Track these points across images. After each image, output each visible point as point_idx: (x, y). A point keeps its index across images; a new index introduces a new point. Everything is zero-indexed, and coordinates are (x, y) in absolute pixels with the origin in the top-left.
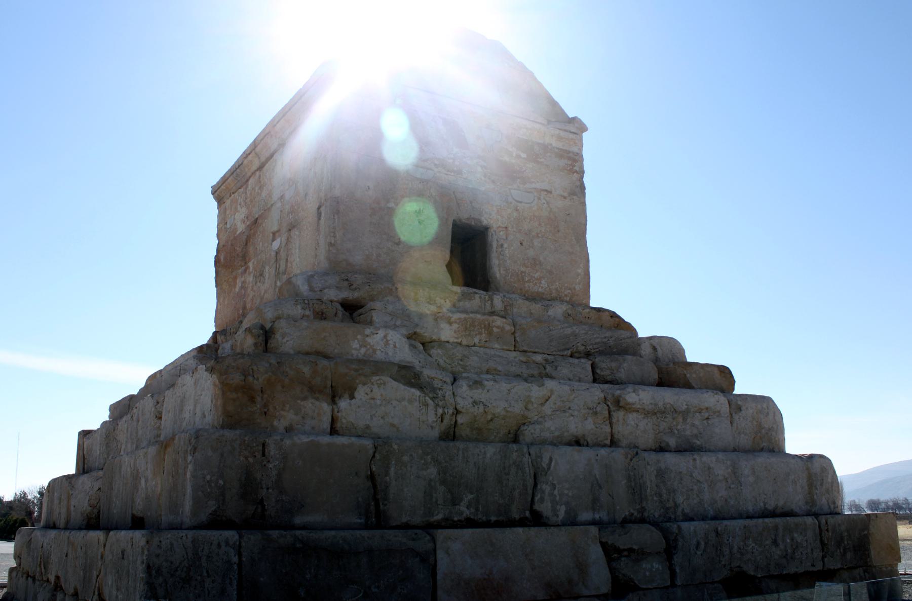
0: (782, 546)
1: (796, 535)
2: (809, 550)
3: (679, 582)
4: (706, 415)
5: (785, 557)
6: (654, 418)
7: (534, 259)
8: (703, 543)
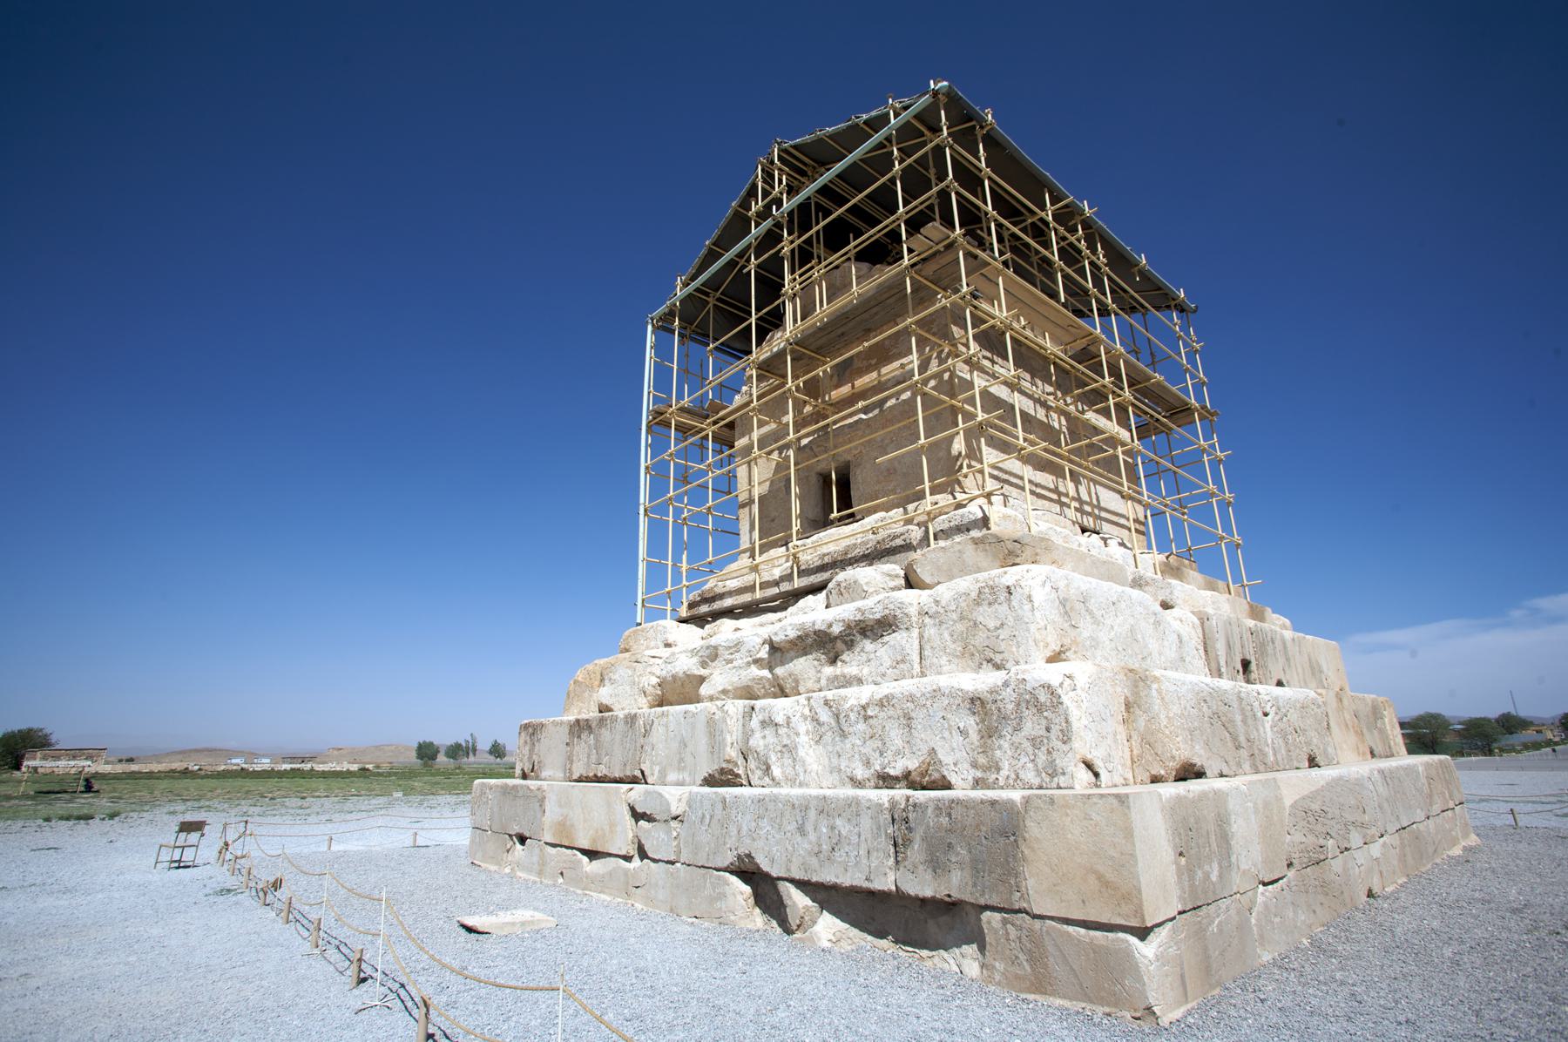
0: (812, 837)
1: (839, 822)
5: (817, 854)
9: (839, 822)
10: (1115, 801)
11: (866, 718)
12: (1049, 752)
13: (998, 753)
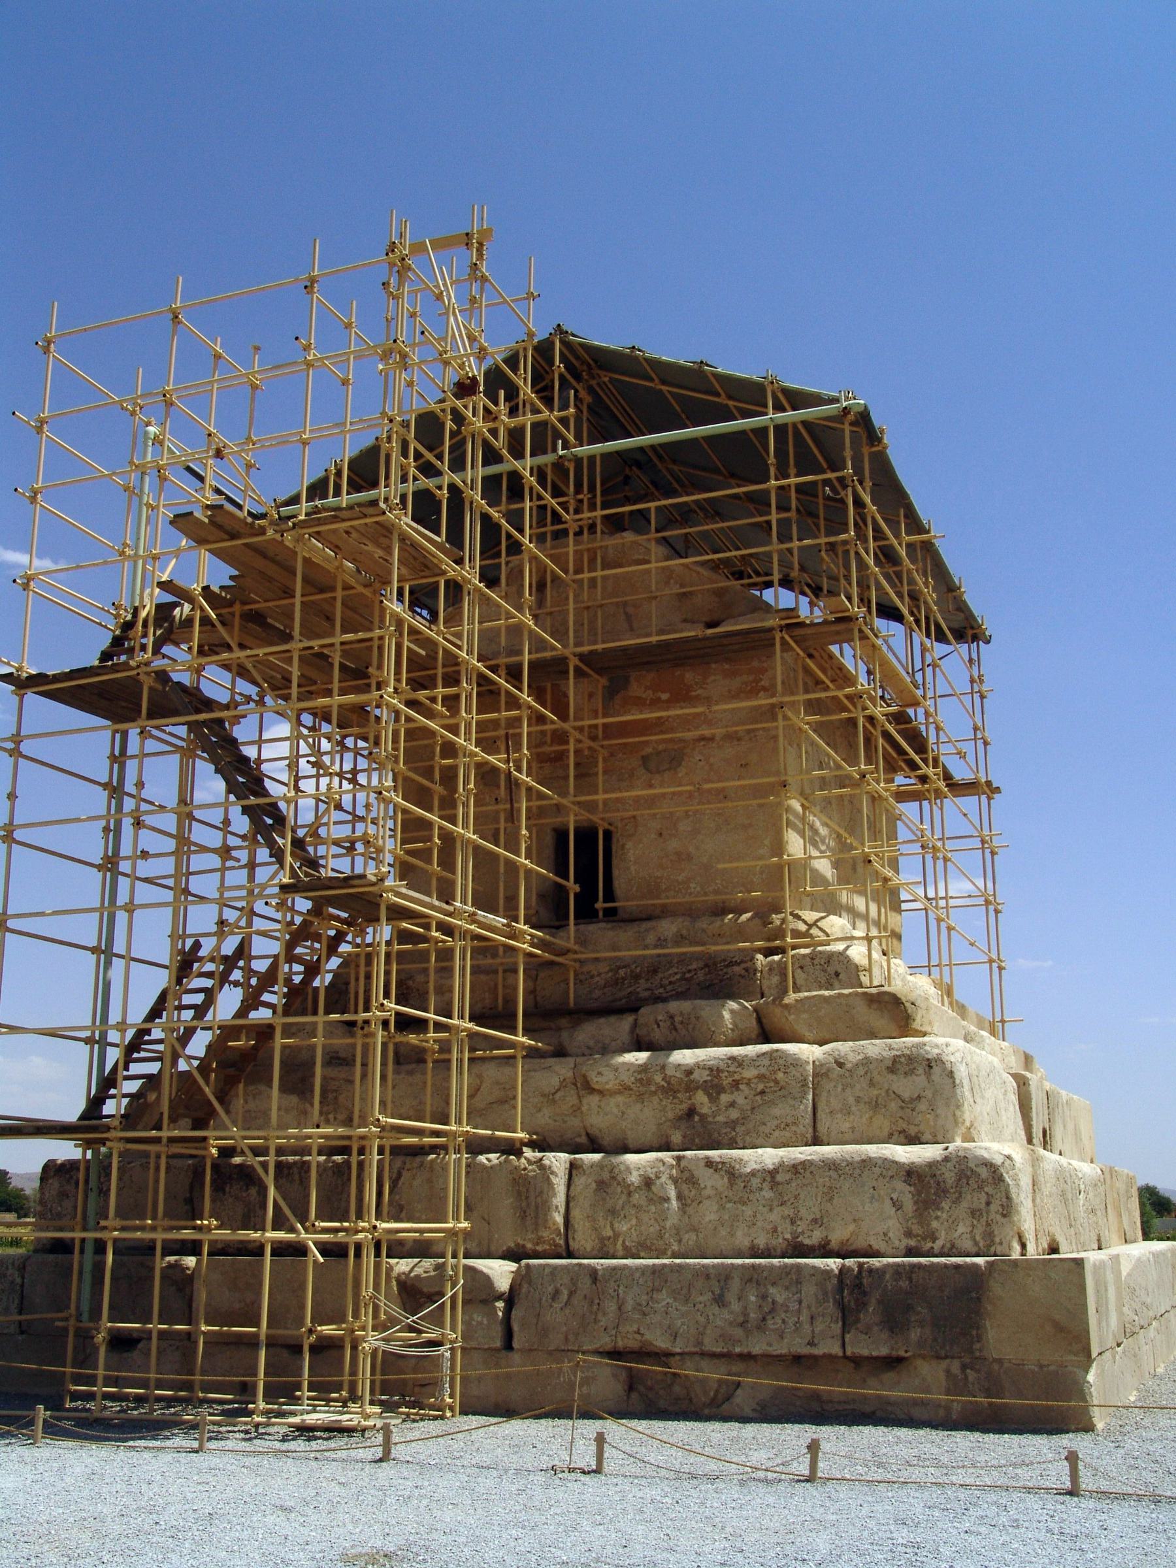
0: (736, 1307)
1: (772, 1290)
2: (804, 1317)
3: (515, 1345)
4: (761, 1087)
6: (655, 1100)
7: (678, 854)
8: (566, 1292)
9: (772, 1290)
10: (1072, 1264)
11: (774, 1184)
12: (988, 1225)
13: (935, 1224)
